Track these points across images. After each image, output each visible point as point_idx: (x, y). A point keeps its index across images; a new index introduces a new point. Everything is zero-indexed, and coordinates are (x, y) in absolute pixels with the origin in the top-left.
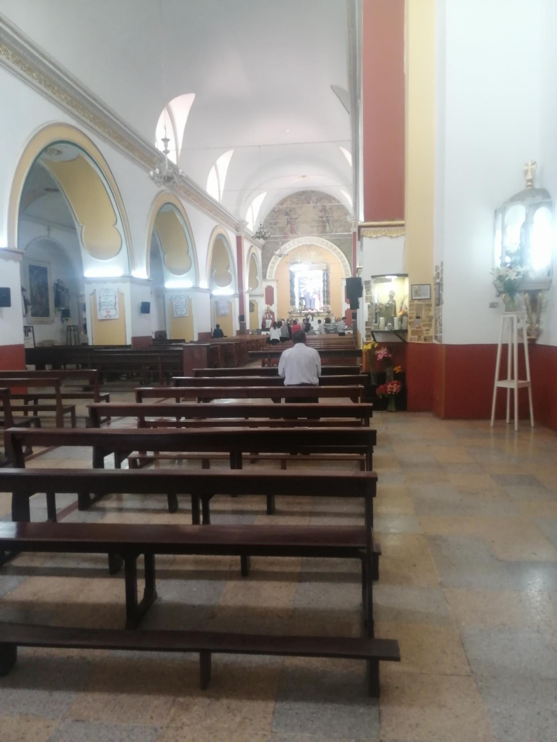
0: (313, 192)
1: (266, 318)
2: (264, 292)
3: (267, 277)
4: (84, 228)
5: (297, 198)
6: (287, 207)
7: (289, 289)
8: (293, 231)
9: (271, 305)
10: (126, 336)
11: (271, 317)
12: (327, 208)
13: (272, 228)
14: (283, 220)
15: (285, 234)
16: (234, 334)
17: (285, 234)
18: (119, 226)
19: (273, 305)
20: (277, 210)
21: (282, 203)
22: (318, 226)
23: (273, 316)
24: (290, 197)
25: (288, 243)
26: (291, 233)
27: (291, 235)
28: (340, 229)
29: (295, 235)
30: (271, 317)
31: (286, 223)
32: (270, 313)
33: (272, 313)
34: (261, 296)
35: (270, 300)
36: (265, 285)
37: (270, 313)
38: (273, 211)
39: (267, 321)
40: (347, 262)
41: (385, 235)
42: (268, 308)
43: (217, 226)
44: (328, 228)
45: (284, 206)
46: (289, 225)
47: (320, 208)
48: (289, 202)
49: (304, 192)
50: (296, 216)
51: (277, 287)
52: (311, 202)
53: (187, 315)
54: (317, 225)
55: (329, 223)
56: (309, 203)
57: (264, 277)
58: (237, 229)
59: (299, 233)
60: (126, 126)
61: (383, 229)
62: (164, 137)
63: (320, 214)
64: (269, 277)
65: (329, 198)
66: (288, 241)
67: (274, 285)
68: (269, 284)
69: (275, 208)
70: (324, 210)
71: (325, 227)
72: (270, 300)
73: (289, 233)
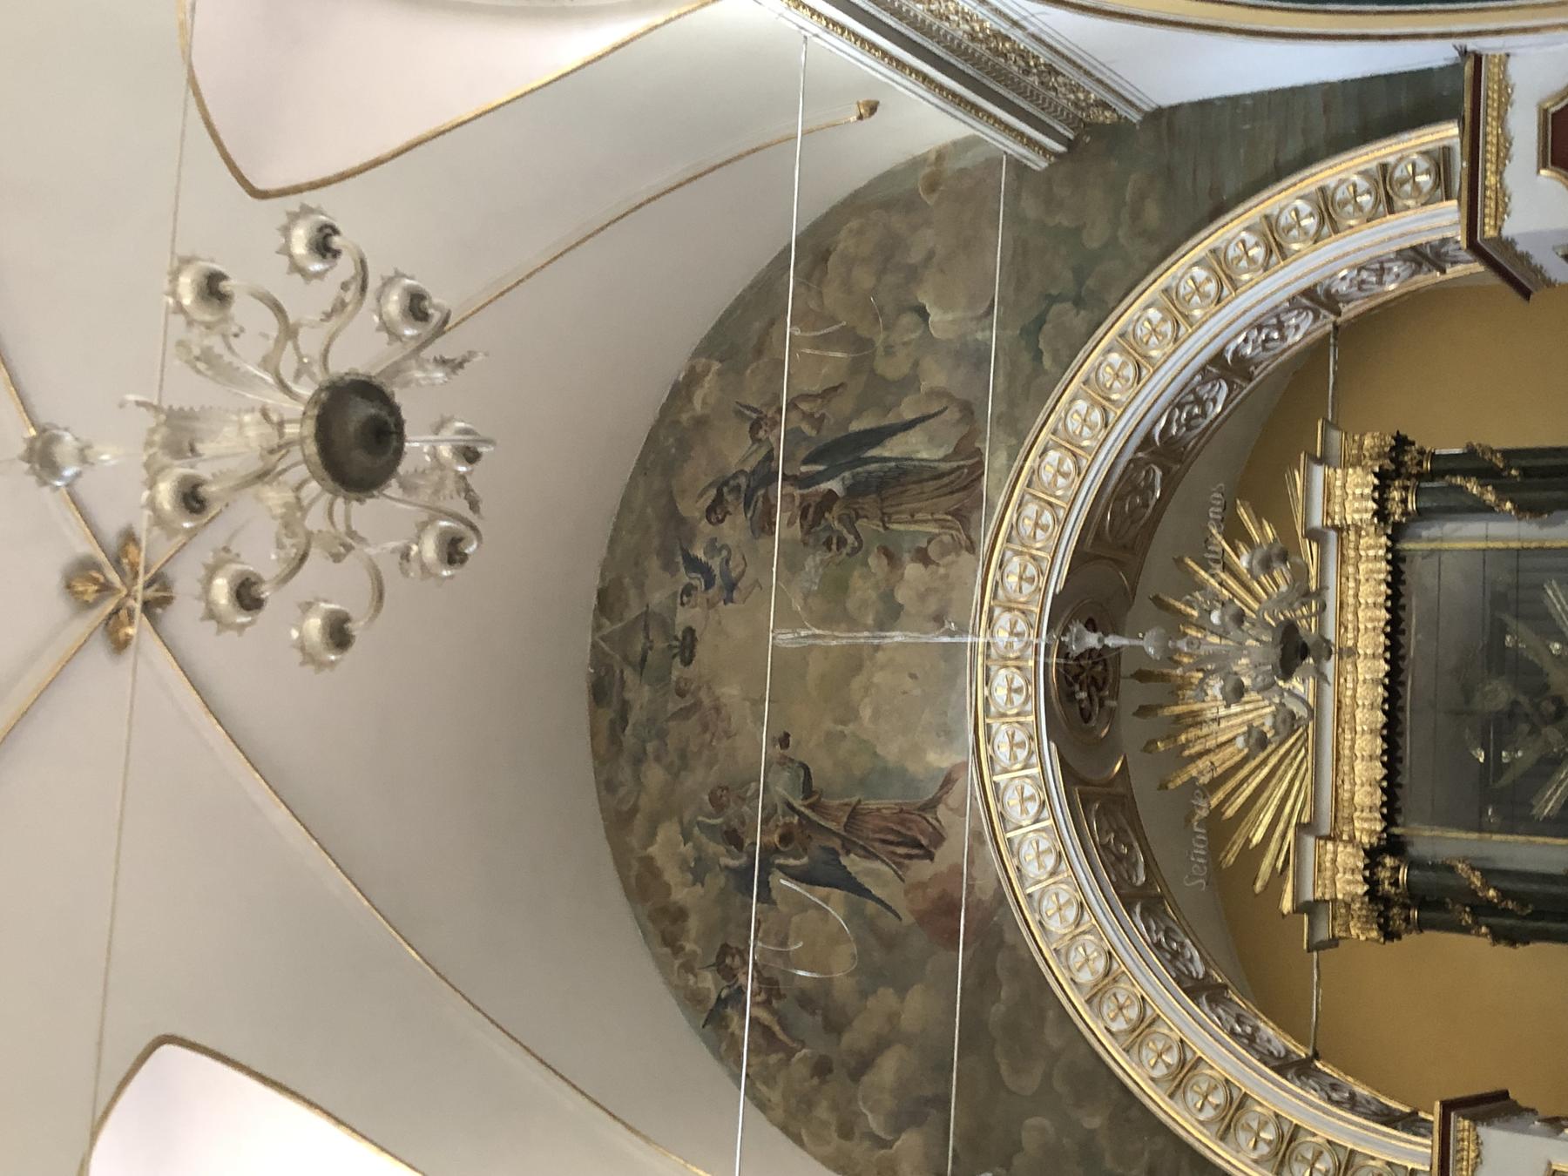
0: (607, 601)
5: (638, 760)
6: (698, 870)
8: (913, 832)
12: (737, 453)
13: (863, 1064)
14: (815, 935)
20: (708, 982)
21: (664, 925)
22: (892, 557)
24: (618, 822)
27: (944, 857)
31: (835, 905)
38: (715, 1019)
44: (918, 447)
45: (682, 893)
46: (854, 864)
47: (734, 529)
48: (666, 848)
49: (600, 692)
50: (784, 787)
52: (684, 617)
54: (876, 563)
56: (687, 646)
59: (939, 759)
65: (670, 438)
69: (690, 999)
73: (922, 870)
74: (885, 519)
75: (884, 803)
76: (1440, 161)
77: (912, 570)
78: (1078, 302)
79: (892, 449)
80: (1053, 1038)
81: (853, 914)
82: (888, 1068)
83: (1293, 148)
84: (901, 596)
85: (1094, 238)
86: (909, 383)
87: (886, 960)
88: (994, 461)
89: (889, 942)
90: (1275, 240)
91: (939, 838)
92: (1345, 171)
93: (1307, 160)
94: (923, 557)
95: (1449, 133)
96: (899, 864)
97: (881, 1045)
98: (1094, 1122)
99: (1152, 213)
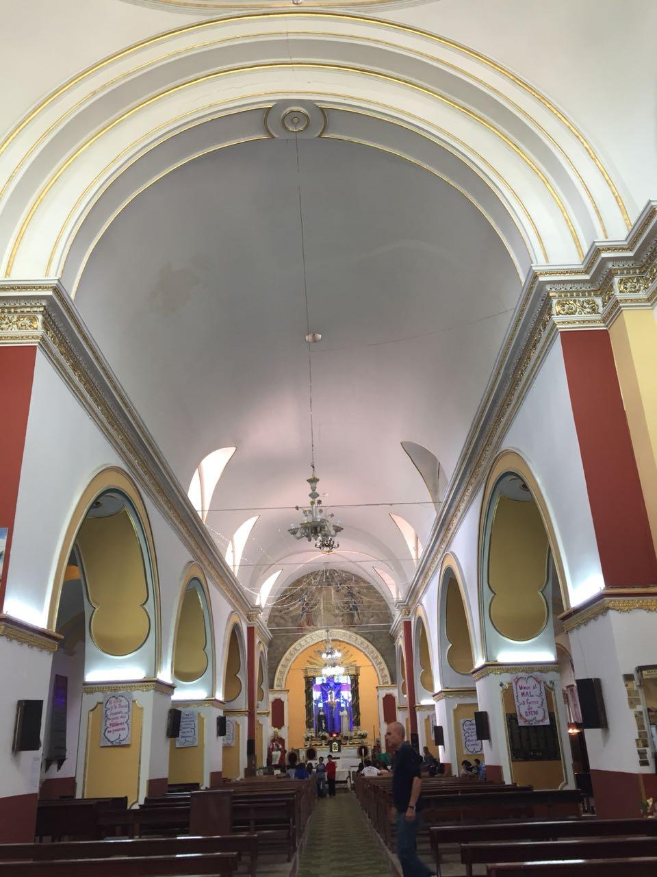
1: (273, 749)
2: (270, 710)
3: (275, 688)
4: (97, 609)
7: (304, 703)
9: (279, 728)
10: (139, 778)
11: (280, 747)
15: (300, 625)
16: (242, 775)
17: (300, 625)
18: (150, 606)
19: (283, 729)
22: (343, 615)
23: (283, 745)
25: (304, 638)
26: (308, 624)
27: (307, 627)
28: (372, 619)
29: (312, 626)
30: (280, 747)
32: (277, 740)
33: (282, 741)
34: (267, 714)
35: (278, 721)
36: (272, 697)
37: (277, 740)
39: (274, 753)
40: (384, 665)
41: (640, 608)
42: (275, 733)
43: (232, 612)
44: (356, 618)
47: (344, 591)
51: (288, 700)
53: (196, 744)
55: (357, 610)
57: (271, 687)
58: (249, 618)
59: (319, 626)
60: (171, 478)
61: (636, 599)
62: (311, 477)
63: (346, 599)
64: (278, 686)
65: (359, 579)
66: (303, 635)
67: (284, 697)
68: (277, 696)
70: (351, 594)
71: (352, 615)
72: (278, 721)
73: (305, 623)
74: (348, 614)
75: (313, 618)
76: (387, 683)
77: (341, 619)
78: (373, 639)
79: (356, 614)
80: (290, 643)
81: (299, 615)
82: (282, 621)
83: (389, 665)
84: (338, 617)
85: (381, 640)
86: (364, 616)
87: (295, 620)
88: (354, 630)
89: (296, 619)
90: (380, 663)
91: (310, 626)
92: (386, 672)
93: (388, 666)
94: (343, 620)
95: (390, 683)
96: (306, 620)
97: (285, 620)
98: (281, 649)
99: (383, 647)
